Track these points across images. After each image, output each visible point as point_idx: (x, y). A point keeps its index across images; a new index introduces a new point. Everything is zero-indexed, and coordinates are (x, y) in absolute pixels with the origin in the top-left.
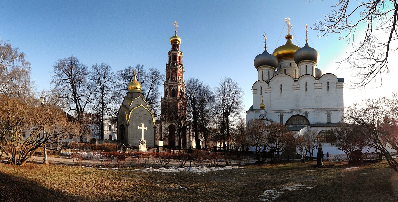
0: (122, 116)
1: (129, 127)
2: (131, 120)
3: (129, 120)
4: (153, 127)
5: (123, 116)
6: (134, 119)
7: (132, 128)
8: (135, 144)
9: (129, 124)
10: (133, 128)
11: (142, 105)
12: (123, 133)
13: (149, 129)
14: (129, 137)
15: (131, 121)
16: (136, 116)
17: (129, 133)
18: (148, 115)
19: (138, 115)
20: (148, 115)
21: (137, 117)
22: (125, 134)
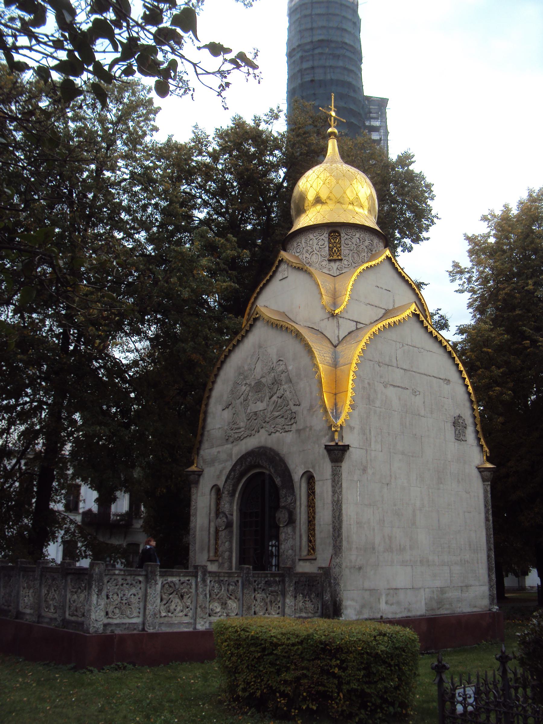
0: (258, 387)
1: (345, 466)
2: (356, 413)
3: (346, 409)
4: (478, 468)
5: (276, 382)
6: (378, 403)
7: (364, 470)
8: (383, 599)
9: (346, 442)
10: (370, 471)
11: (418, 312)
12: (282, 516)
13: (458, 482)
14: (345, 544)
15: (356, 423)
16: (385, 387)
17: (344, 511)
18: (447, 381)
19: (397, 376)
20: (447, 381)
21: (391, 392)
22: (291, 521)
